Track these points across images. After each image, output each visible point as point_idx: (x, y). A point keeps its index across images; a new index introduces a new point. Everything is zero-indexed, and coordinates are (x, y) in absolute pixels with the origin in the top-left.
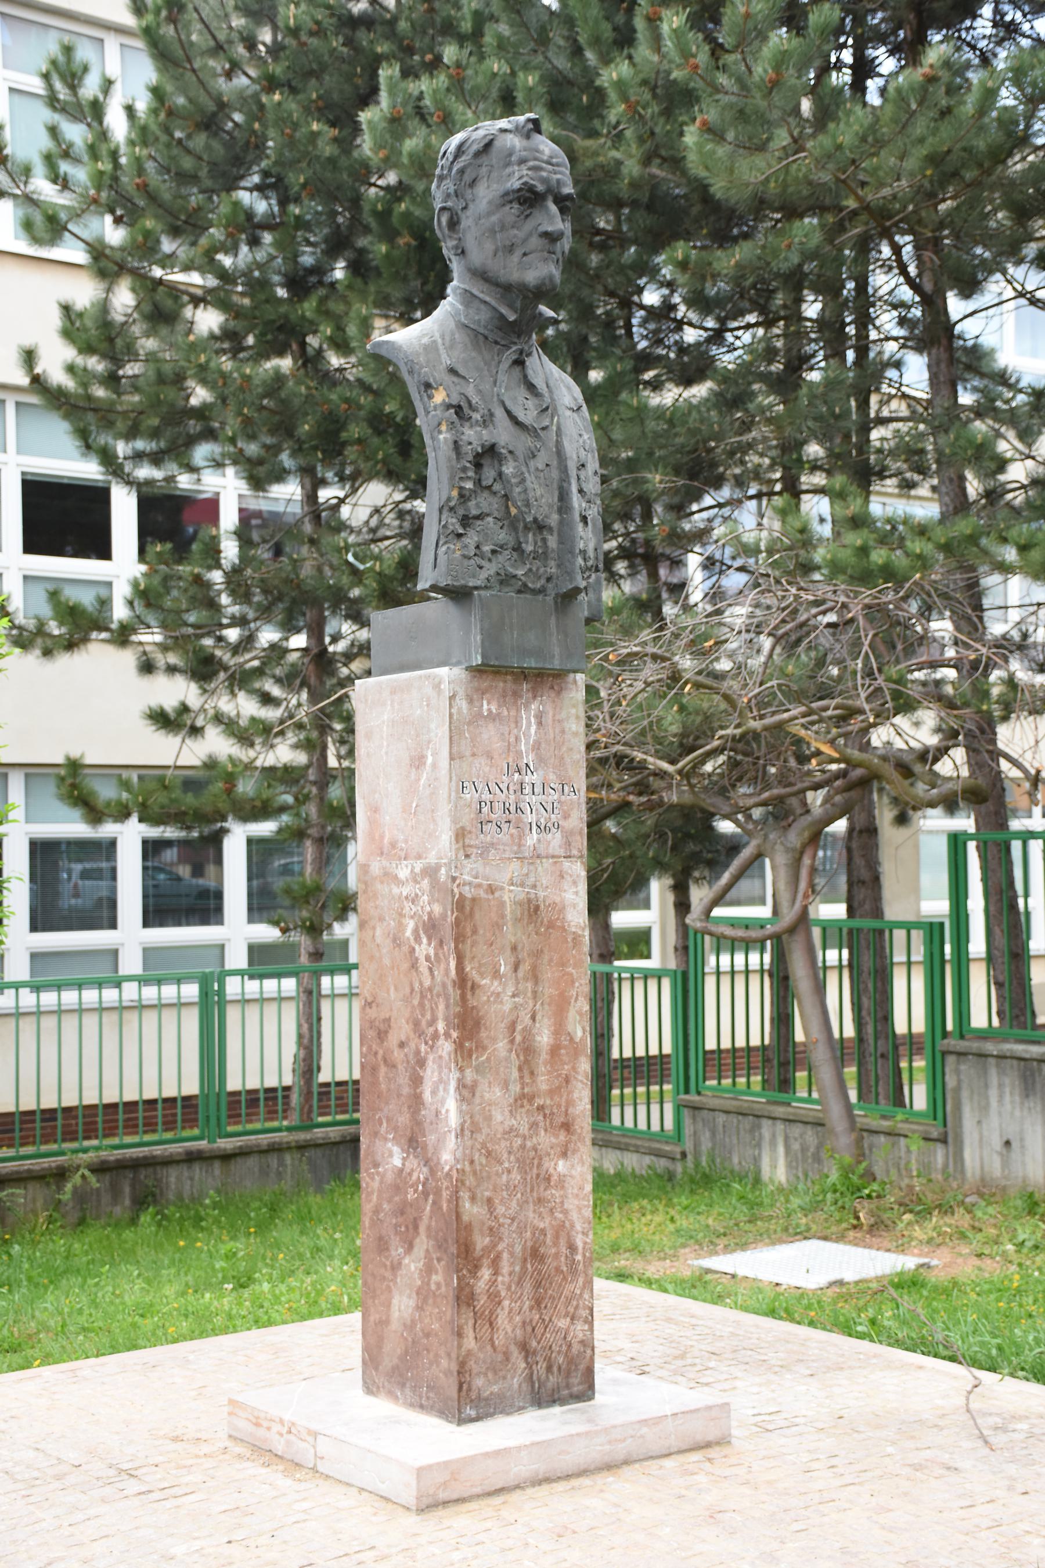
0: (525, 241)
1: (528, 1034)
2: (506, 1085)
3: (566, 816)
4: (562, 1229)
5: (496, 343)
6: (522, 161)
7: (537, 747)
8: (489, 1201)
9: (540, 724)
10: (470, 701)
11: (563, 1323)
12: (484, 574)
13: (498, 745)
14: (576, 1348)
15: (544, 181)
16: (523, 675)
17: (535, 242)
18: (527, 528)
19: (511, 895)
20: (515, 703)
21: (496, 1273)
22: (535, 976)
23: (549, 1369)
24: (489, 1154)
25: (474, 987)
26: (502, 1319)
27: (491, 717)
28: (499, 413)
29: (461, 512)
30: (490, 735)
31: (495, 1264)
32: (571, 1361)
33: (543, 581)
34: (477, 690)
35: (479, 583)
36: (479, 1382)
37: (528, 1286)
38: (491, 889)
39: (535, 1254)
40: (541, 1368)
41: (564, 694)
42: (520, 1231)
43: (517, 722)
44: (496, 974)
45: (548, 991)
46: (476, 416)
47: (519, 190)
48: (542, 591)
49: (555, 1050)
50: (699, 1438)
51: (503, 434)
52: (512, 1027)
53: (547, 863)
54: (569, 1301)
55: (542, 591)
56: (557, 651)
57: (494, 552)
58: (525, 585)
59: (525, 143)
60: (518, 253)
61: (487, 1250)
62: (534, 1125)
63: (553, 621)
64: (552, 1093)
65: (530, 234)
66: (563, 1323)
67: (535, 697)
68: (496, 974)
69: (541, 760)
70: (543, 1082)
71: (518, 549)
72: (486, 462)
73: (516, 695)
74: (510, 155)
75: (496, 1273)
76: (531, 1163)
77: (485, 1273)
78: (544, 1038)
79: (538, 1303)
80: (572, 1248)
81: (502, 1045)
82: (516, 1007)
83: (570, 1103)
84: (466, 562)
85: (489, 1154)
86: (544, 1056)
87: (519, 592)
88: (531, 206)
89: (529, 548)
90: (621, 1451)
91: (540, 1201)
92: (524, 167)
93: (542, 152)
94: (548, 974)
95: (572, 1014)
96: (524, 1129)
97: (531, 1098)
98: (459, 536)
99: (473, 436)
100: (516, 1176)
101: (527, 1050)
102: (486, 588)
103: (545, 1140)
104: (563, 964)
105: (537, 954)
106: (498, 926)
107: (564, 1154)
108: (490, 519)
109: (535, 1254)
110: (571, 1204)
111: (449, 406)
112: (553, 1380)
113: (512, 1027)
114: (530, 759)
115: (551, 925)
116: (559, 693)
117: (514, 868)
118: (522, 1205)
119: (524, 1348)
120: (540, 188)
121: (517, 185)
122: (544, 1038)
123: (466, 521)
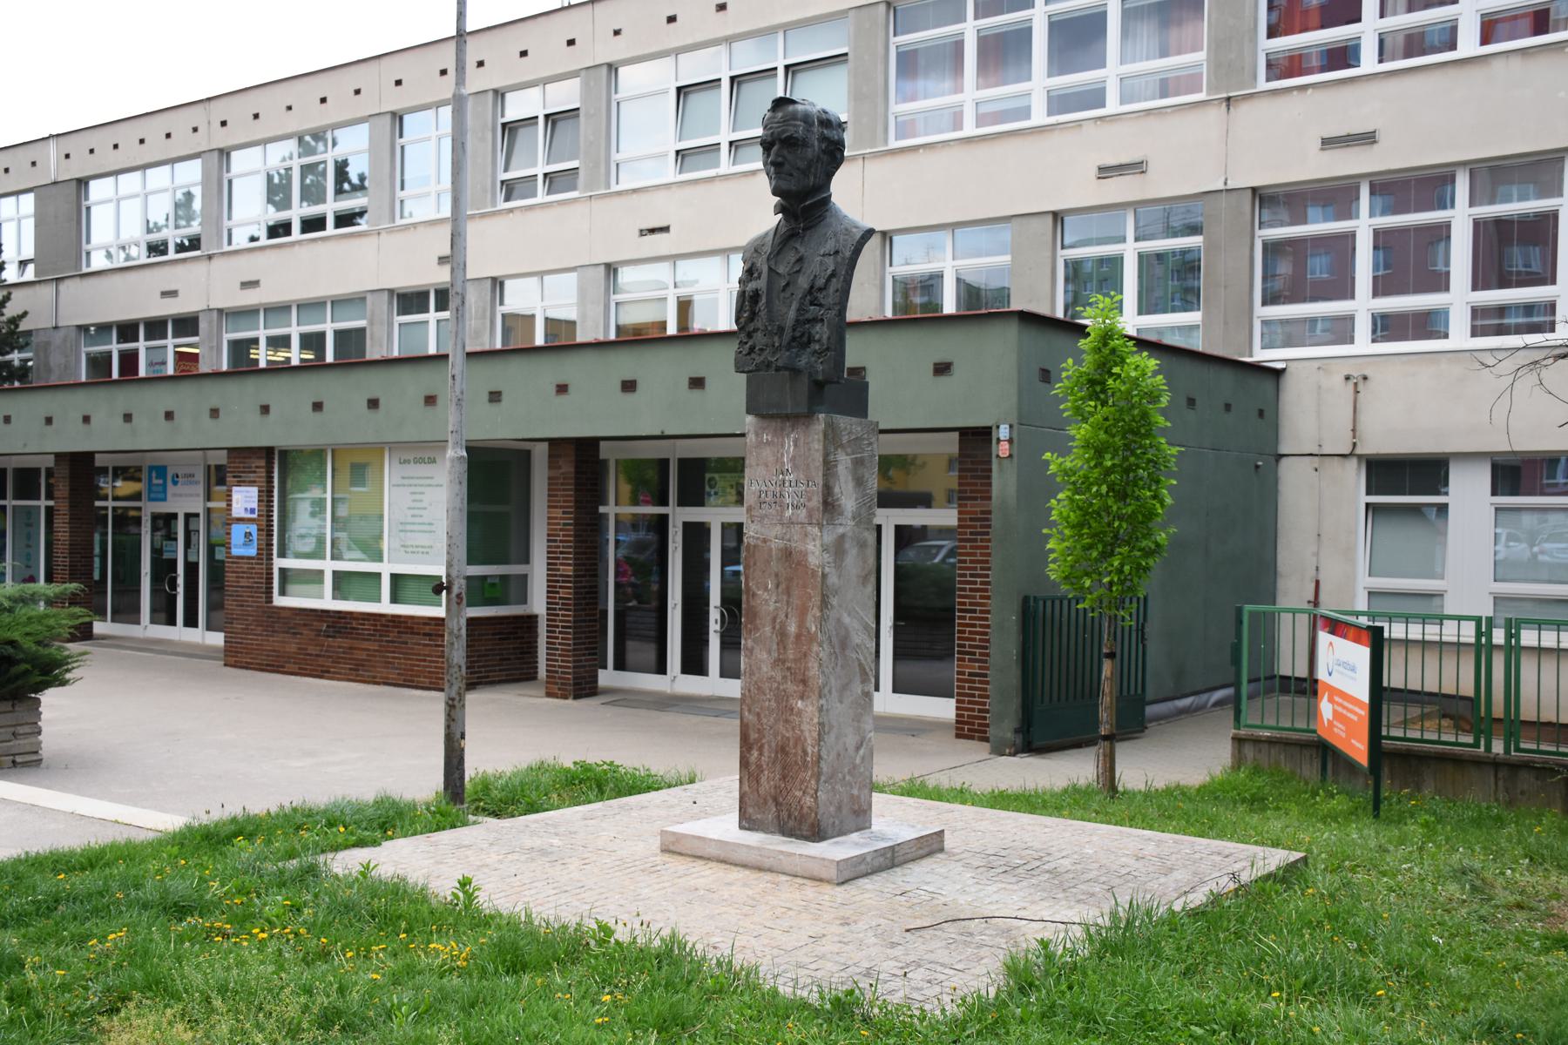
1: (783, 626)
2: (769, 652)
3: (809, 500)
4: (799, 740)
7: (793, 459)
8: (758, 715)
9: (796, 445)
11: (799, 794)
13: (771, 459)
14: (805, 810)
16: (787, 417)
19: (776, 544)
21: (761, 754)
22: (788, 592)
23: (789, 816)
24: (759, 688)
25: (754, 595)
26: (763, 780)
27: (768, 443)
30: (767, 453)
31: (761, 749)
32: (802, 816)
36: (750, 810)
37: (778, 767)
38: (765, 541)
39: (783, 749)
40: (784, 814)
42: (775, 735)
43: (783, 446)
44: (766, 589)
45: (796, 601)
49: (798, 636)
50: (815, 874)
52: (774, 620)
53: (798, 527)
54: (802, 782)
61: (758, 740)
62: (784, 677)
64: (795, 661)
66: (799, 794)
68: (766, 589)
69: (795, 467)
70: (791, 654)
73: (782, 429)
75: (761, 754)
76: (782, 698)
77: (755, 753)
78: (792, 629)
79: (784, 778)
80: (805, 753)
81: (768, 629)
82: (776, 609)
83: (807, 669)
85: (759, 688)
86: (792, 639)
90: (767, 863)
91: (787, 721)
94: (796, 592)
95: (810, 617)
96: (779, 678)
97: (784, 662)
99: (751, 286)
100: (773, 704)
101: (782, 634)
103: (791, 687)
104: (805, 586)
105: (790, 580)
106: (768, 562)
107: (802, 698)
109: (783, 749)
110: (805, 727)
112: (791, 823)
113: (774, 620)
114: (788, 466)
115: (799, 563)
117: (778, 530)
118: (777, 721)
119: (775, 799)
122: (792, 629)
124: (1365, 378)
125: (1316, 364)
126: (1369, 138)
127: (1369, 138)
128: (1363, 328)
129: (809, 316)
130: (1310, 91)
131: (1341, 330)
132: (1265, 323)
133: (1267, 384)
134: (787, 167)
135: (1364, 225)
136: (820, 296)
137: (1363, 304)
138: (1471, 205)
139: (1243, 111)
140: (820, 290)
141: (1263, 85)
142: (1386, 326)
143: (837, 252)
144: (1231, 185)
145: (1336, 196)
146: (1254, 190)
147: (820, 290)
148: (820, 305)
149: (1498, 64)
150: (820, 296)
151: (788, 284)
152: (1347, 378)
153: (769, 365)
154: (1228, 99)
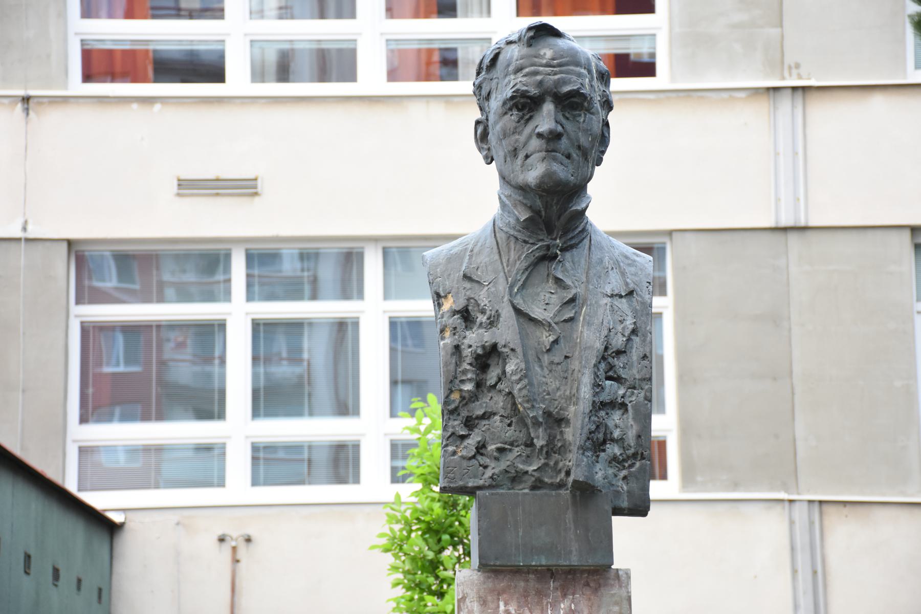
0: (525, 144)
5: (525, 242)
6: (518, 70)
10: (484, 602)
12: (489, 473)
15: (540, 83)
16: (548, 573)
17: (535, 143)
18: (537, 424)
20: (539, 603)
28: (507, 313)
29: (464, 413)
33: (563, 475)
34: (492, 591)
35: (481, 482)
41: (603, 590)
46: (481, 318)
47: (512, 98)
48: (561, 485)
51: (506, 332)
55: (561, 485)
56: (574, 547)
57: (501, 450)
58: (539, 480)
59: (525, 50)
60: (521, 156)
63: (569, 515)
65: (530, 137)
67: (564, 596)
71: (530, 444)
72: (493, 361)
74: (508, 65)
84: (465, 463)
87: (534, 488)
88: (531, 110)
89: (539, 443)
92: (520, 75)
93: (543, 57)
98: (463, 438)
99: (475, 339)
102: (491, 487)
108: (497, 418)
111: (455, 312)
116: (596, 590)
120: (533, 91)
121: (510, 95)
123: (470, 423)
124: (248, 540)
125: (173, 517)
126: (246, 188)
127: (246, 188)
128: (238, 465)
129: (605, 397)
130: (157, 107)
131: (207, 464)
132: (83, 451)
133: (100, 541)
134: (564, 140)
135: (238, 313)
136: (619, 363)
137: (239, 428)
138: (386, 296)
139: (50, 120)
140: (619, 353)
141: (77, 86)
142: (271, 463)
143: (631, 293)
144: (31, 234)
145: (205, 264)
146: (70, 243)
147: (619, 353)
148: (618, 379)
149: (417, 110)
150: (619, 363)
151: (556, 342)
152: (222, 540)
153: (516, 478)
154: (26, 100)
